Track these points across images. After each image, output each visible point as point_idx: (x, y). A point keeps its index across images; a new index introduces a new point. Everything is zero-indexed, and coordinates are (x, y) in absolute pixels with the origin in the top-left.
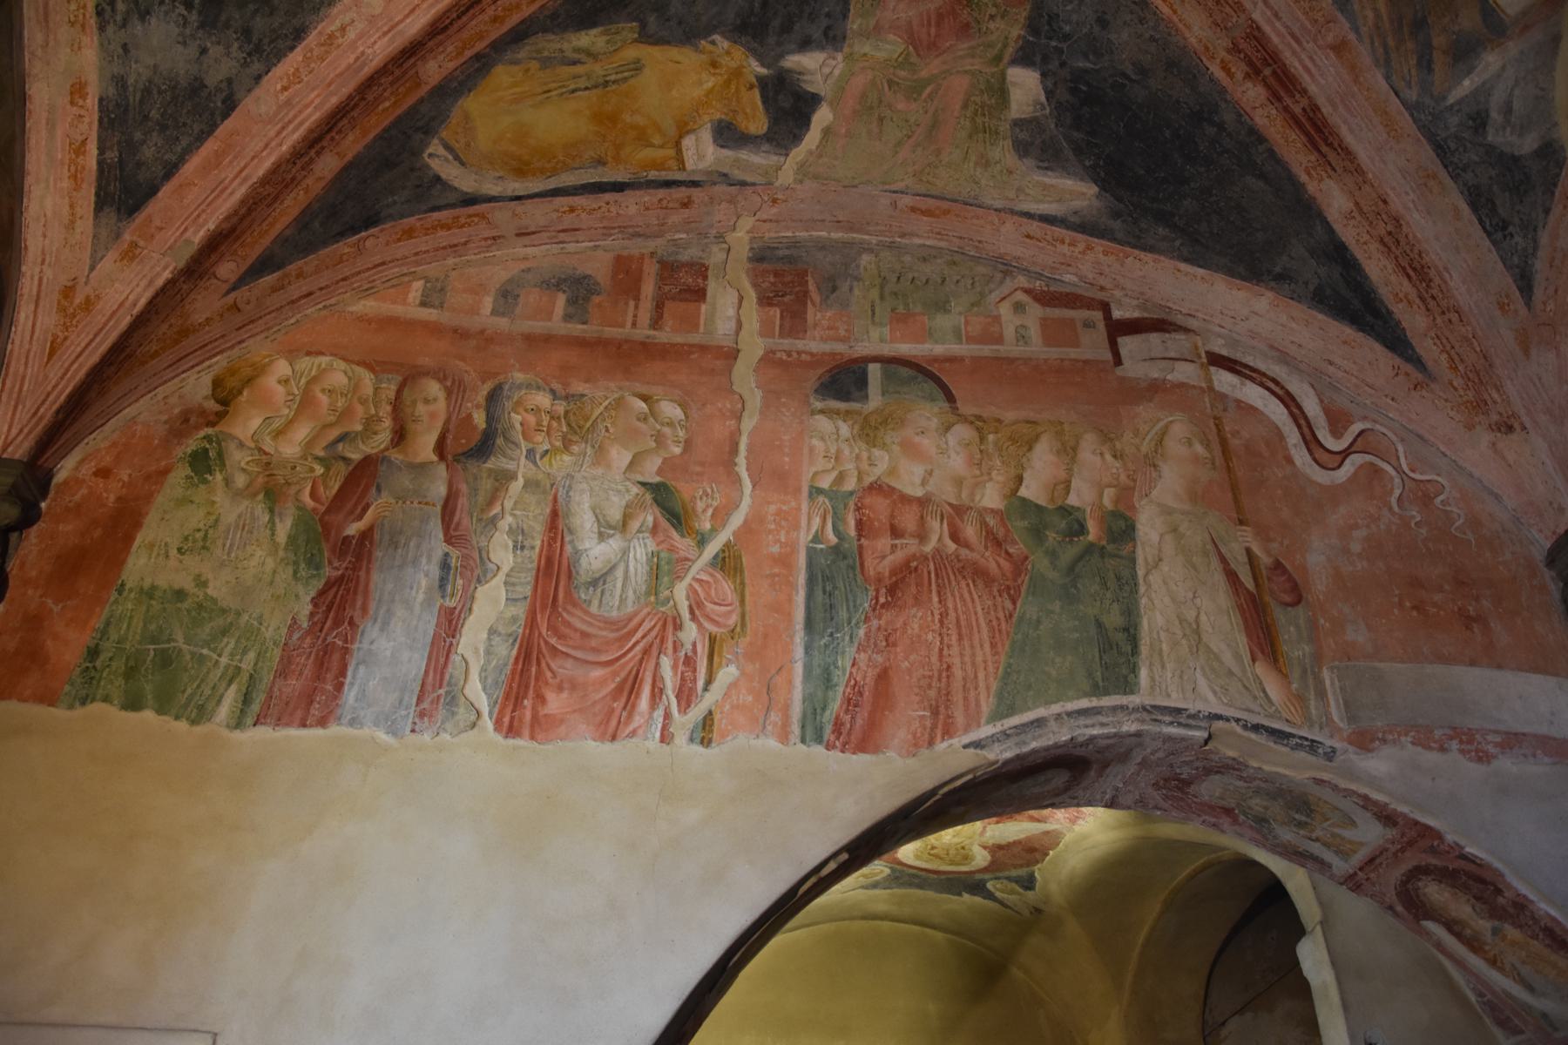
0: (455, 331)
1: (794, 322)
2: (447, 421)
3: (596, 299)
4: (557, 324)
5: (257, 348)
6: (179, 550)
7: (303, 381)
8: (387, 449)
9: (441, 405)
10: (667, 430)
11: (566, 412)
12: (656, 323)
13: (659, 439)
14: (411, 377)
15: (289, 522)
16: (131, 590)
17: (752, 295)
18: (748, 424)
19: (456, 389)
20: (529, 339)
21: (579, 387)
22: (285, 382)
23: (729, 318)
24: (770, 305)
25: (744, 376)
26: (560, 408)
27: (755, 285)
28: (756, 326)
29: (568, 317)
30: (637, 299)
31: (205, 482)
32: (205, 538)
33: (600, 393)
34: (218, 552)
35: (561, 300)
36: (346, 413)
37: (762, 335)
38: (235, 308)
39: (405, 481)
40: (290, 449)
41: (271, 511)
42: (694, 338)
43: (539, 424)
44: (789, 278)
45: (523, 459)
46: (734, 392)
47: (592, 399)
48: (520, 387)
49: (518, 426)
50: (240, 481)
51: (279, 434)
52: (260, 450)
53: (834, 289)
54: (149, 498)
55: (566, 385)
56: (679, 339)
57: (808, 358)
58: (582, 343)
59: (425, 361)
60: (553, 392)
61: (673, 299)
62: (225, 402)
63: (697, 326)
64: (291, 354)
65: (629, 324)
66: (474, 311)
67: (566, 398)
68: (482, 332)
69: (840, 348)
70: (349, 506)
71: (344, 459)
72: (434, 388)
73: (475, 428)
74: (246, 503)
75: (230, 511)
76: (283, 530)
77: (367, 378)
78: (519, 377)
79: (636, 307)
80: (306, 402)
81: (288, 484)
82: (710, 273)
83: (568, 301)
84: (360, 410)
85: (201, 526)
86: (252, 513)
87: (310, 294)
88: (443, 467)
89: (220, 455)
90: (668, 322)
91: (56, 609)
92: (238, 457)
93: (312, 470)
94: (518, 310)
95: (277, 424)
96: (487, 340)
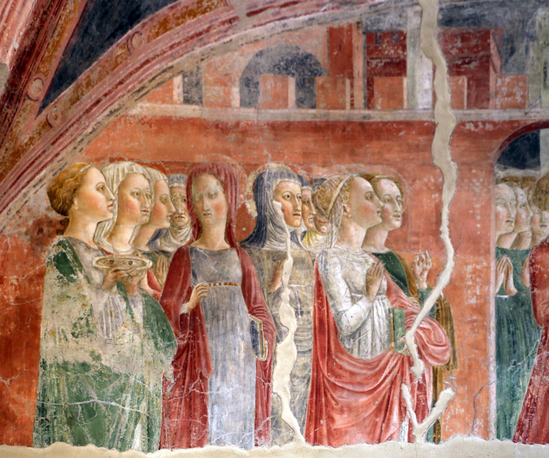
0: (217, 126)
1: (478, 92)
2: (229, 213)
3: (319, 81)
4: (293, 112)
5: (71, 158)
6: (73, 334)
7: (115, 187)
8: (191, 242)
9: (221, 198)
10: (388, 206)
11: (313, 196)
12: (369, 103)
13: (383, 213)
14: (194, 174)
15: (140, 307)
16: (51, 366)
17: (443, 63)
18: (448, 196)
19: (229, 183)
20: (274, 127)
21: (320, 172)
22: (101, 189)
23: (426, 91)
24: (459, 74)
25: (442, 151)
26: (308, 193)
27: (446, 52)
28: (448, 97)
29: (300, 102)
30: (351, 77)
31: (72, 280)
32: (88, 324)
33: (335, 175)
34: (100, 333)
35: (292, 82)
36: (155, 213)
37: (453, 107)
38: (47, 125)
39: (210, 266)
40: (123, 247)
41: (126, 299)
42: (400, 115)
43: (295, 208)
44: (473, 42)
45: (289, 240)
46: (434, 167)
47: (330, 182)
48: (275, 176)
49: (280, 212)
50: (97, 277)
51: (111, 235)
52: (102, 250)
53: (513, 51)
54: (38, 296)
55: (309, 170)
56: (388, 117)
57: (489, 127)
58: (317, 129)
59: (201, 158)
60: (300, 178)
61: (380, 74)
62: (63, 212)
63: (400, 102)
64: (100, 161)
65: (348, 105)
66: (226, 104)
67: (311, 182)
68: (237, 124)
69: (516, 115)
70: (178, 290)
71: (165, 253)
72: (212, 183)
73: (250, 216)
74: (106, 295)
75: (100, 302)
76: (139, 311)
77: (161, 177)
78: (273, 166)
79: (352, 85)
80: (123, 206)
81: (131, 277)
82: (408, 42)
83: (297, 84)
84: (163, 208)
85: (82, 315)
86: (113, 302)
87: (98, 102)
88: (234, 252)
89: (76, 257)
90: (379, 101)
91: (7, 382)
92: (89, 258)
93: (144, 264)
94: (261, 99)
95: (108, 226)
96: (243, 131)
